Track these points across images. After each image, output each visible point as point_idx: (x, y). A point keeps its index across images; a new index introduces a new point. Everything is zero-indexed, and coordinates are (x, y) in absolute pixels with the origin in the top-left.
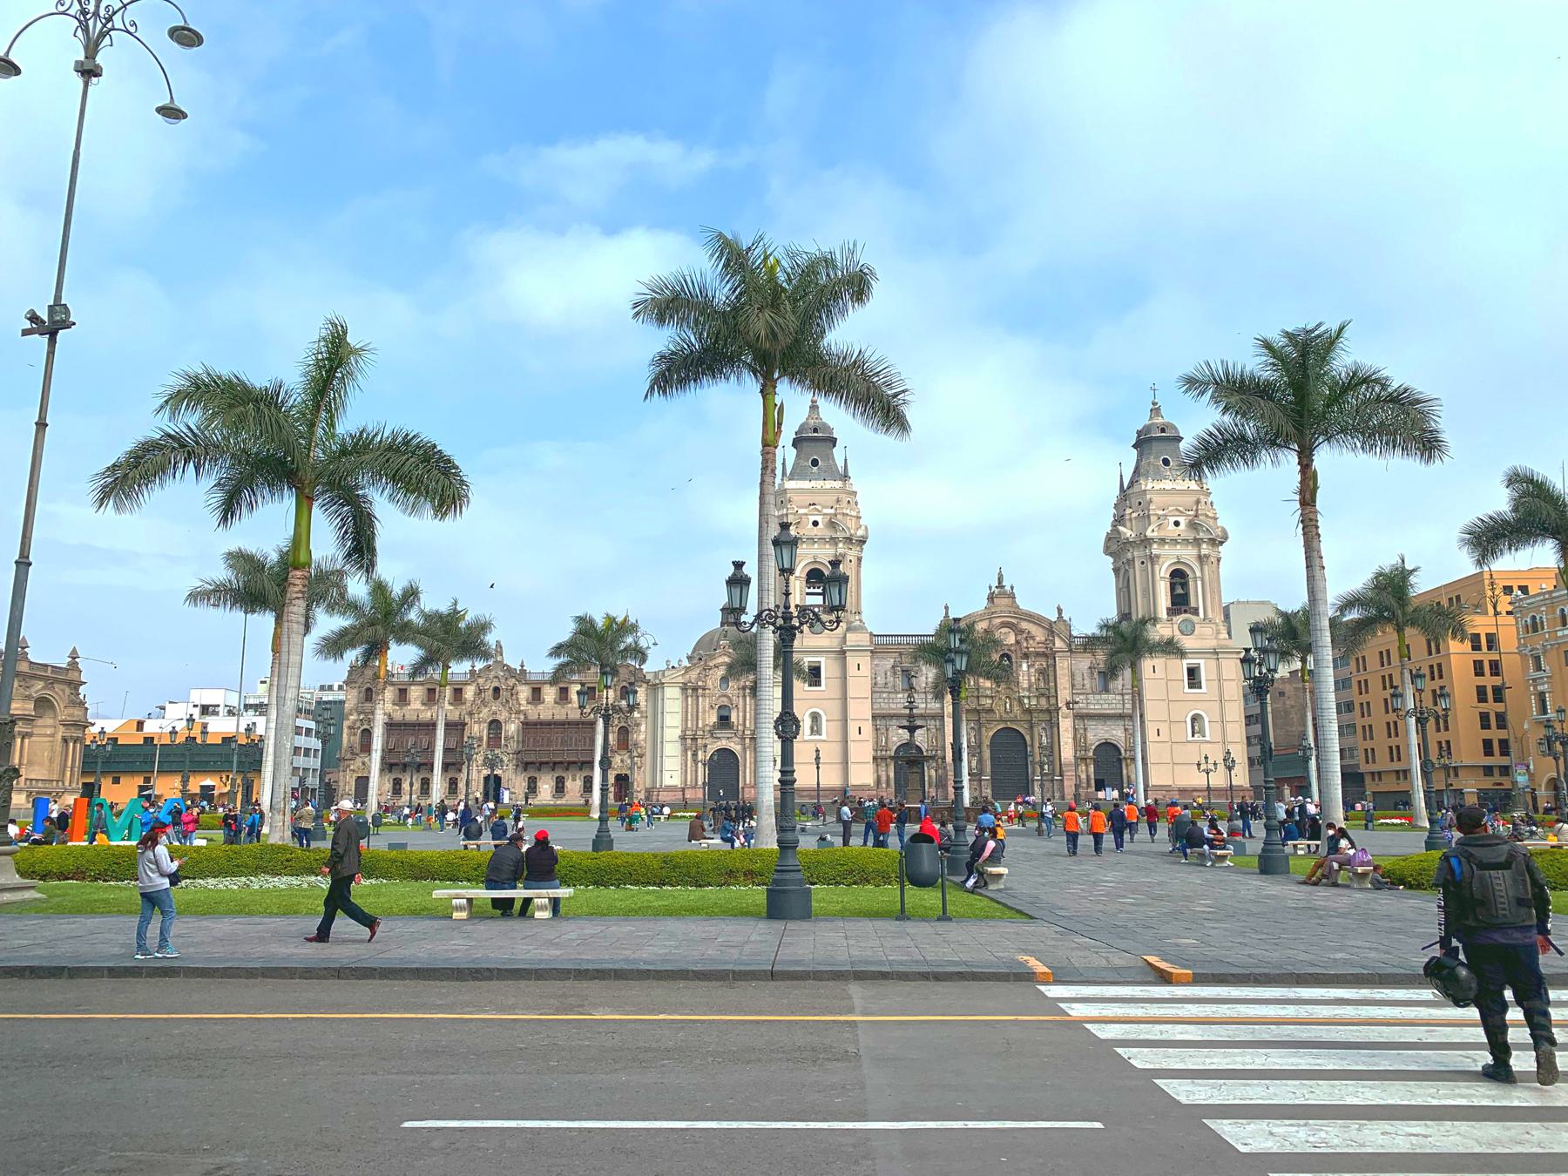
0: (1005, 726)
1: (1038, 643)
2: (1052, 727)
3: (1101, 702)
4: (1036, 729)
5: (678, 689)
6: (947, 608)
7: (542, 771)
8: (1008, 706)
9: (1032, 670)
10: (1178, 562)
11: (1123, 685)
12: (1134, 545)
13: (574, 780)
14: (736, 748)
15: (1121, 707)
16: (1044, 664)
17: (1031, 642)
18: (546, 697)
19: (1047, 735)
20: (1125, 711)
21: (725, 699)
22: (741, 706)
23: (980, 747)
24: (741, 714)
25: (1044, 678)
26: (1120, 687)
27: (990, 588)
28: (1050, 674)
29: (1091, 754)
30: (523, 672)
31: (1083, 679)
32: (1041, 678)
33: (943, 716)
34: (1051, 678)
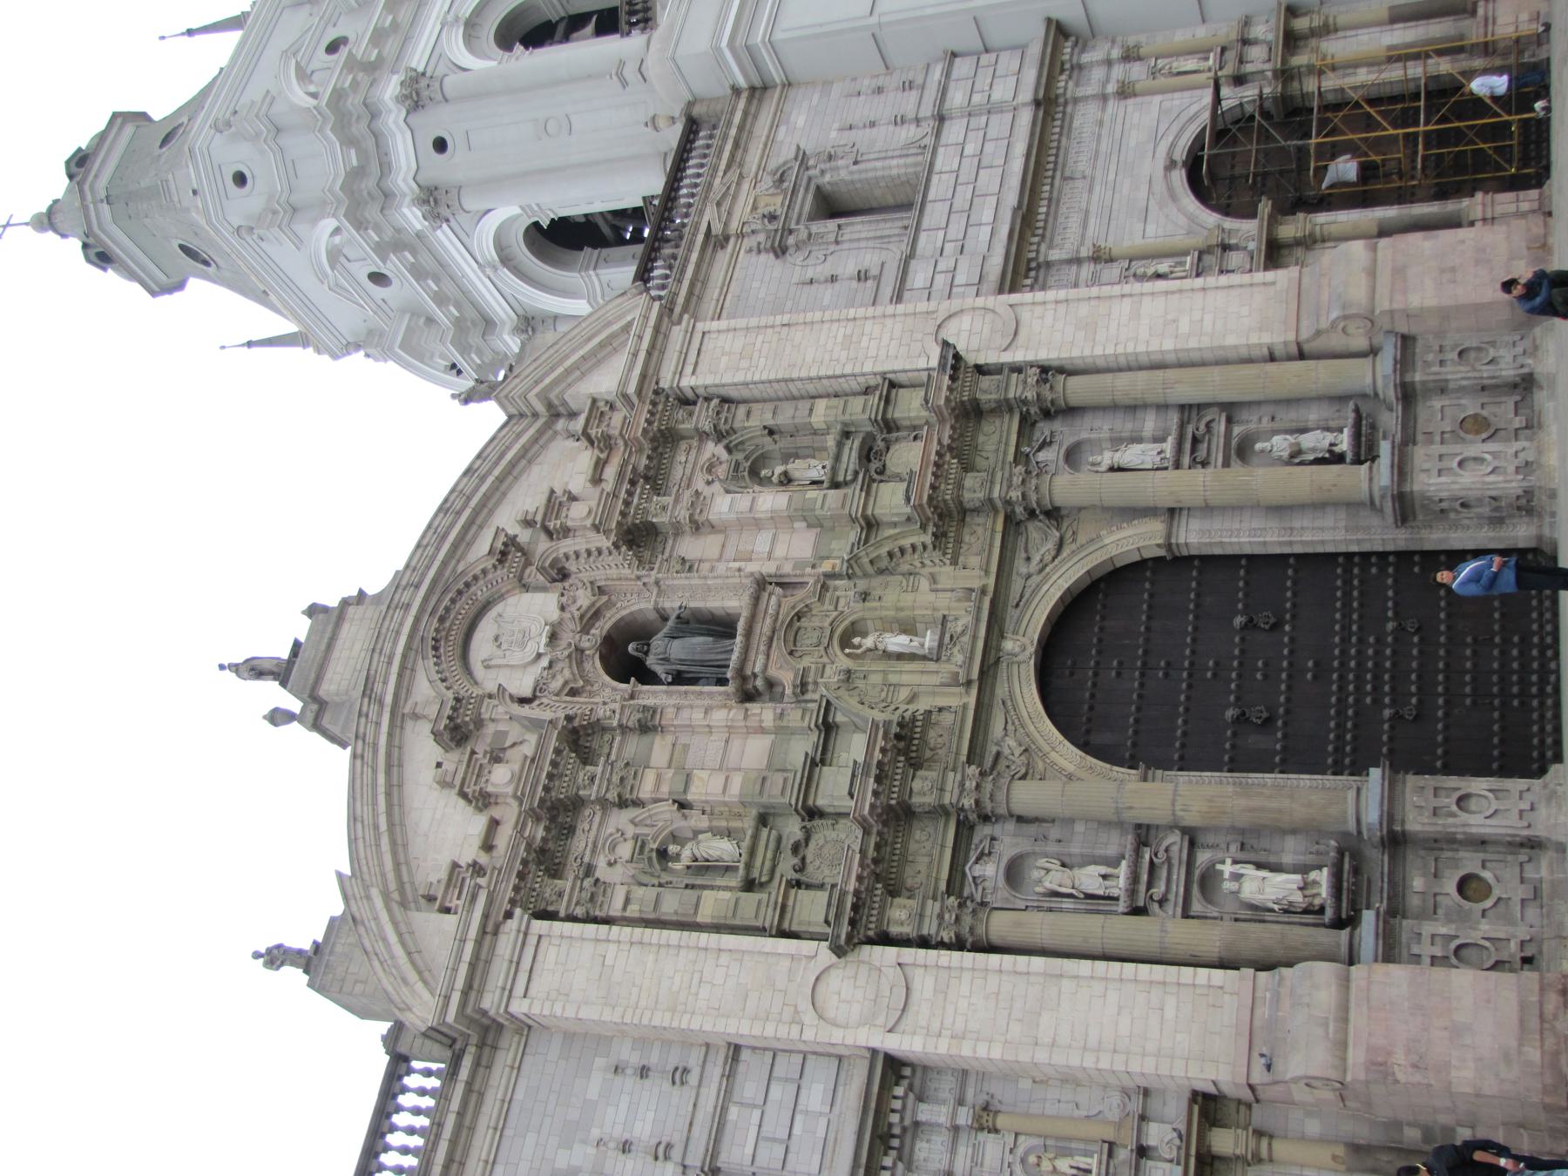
0: (1028, 671)
1: (597, 480)
2: (1071, 411)
3: (965, 193)
4: (1066, 487)
6: (276, 957)
8: (897, 642)
9: (723, 505)
10: (471, 25)
11: (899, 121)
12: (369, 184)
15: (1000, 124)
16: (713, 449)
17: (577, 514)
19: (1117, 442)
20: (1027, 95)
23: (1144, 835)
25: (787, 457)
26: (909, 133)
27: (278, 717)
28: (770, 422)
29: (1248, 231)
31: (833, 279)
32: (779, 469)
33: (893, 1067)
34: (786, 416)
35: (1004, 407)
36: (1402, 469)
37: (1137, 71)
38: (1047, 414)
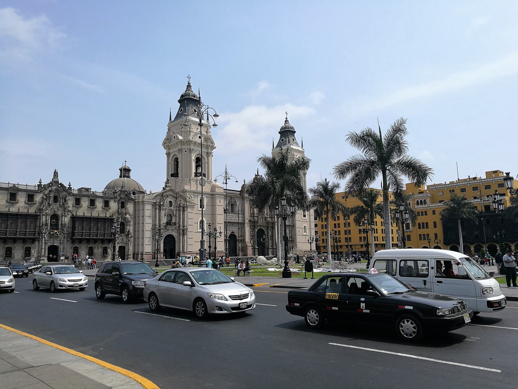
5: (151, 205)
6: (244, 181)
7: (81, 244)
13: (98, 249)
14: (175, 234)
18: (83, 204)
21: (170, 211)
22: (177, 215)
24: (177, 219)
30: (70, 188)
35: (273, 225)
36: (270, 248)
37: (291, 231)
38: (272, 228)
